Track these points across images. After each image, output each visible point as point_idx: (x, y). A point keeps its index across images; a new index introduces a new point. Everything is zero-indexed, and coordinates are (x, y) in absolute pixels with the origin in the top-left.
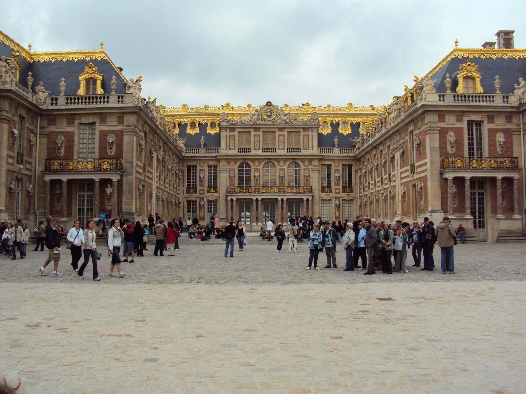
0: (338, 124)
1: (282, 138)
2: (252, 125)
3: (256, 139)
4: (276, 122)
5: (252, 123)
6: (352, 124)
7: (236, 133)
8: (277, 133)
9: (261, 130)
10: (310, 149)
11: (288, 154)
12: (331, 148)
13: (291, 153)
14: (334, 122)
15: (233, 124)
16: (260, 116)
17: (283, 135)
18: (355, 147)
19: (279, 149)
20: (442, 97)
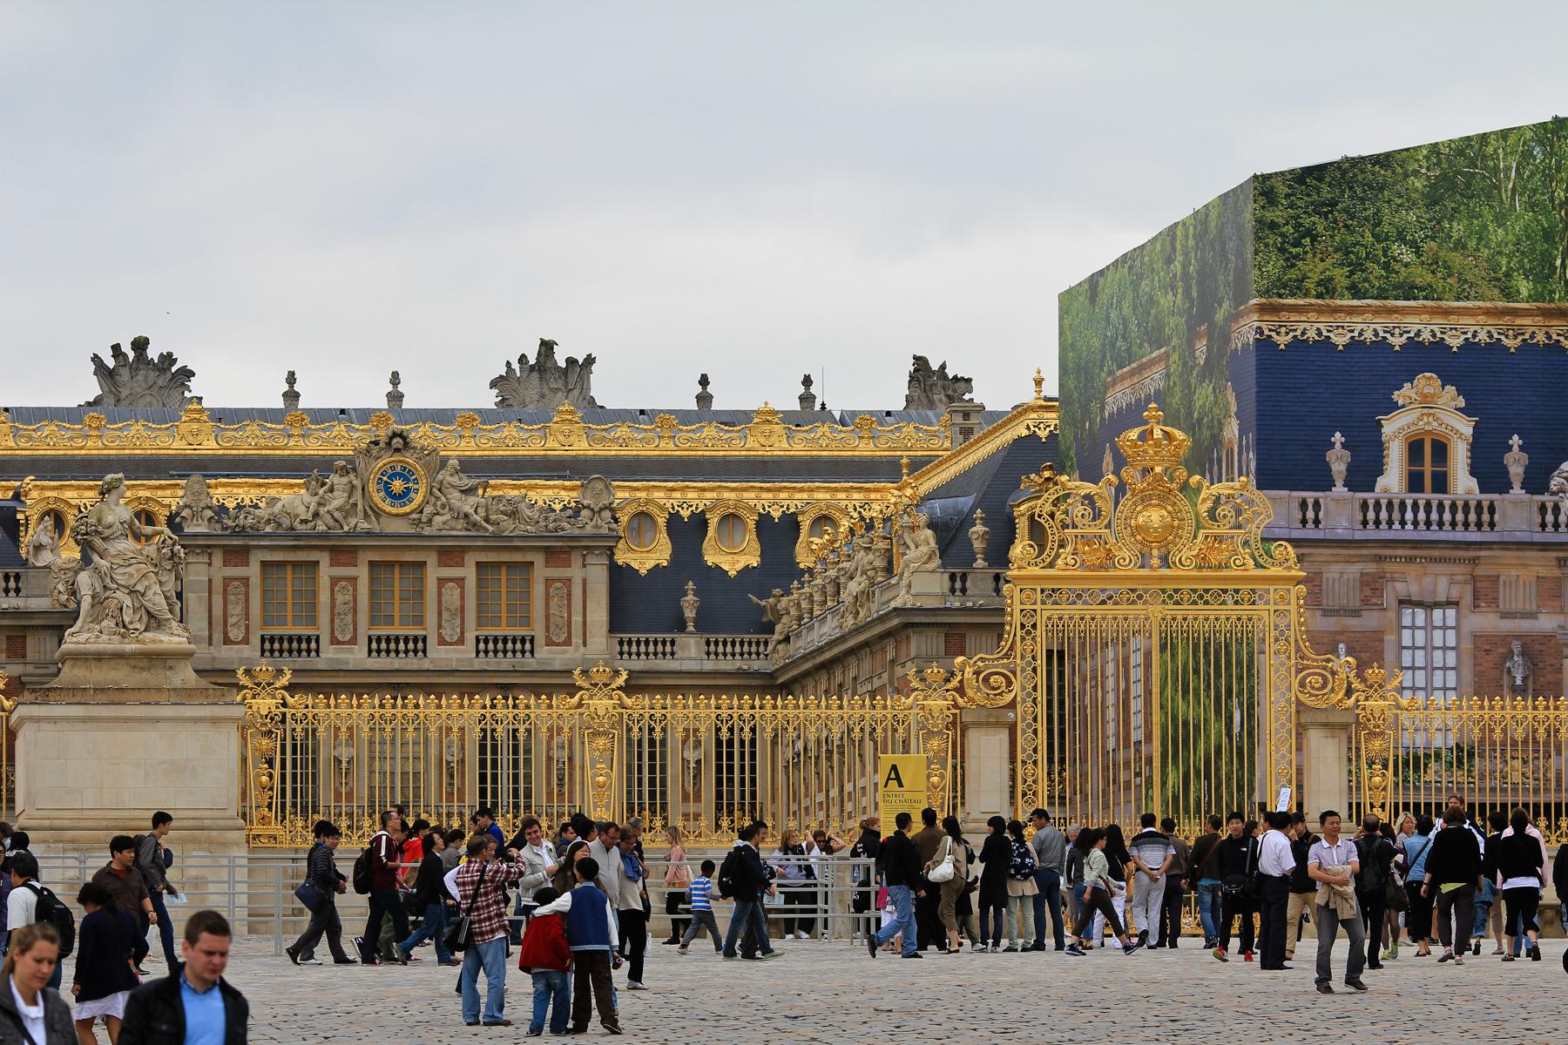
0: (700, 521)
1: (452, 595)
2: (321, 536)
3: (340, 598)
4: (430, 521)
5: (321, 528)
6: (764, 522)
7: (253, 571)
8: (433, 572)
9: (364, 558)
10: (577, 639)
11: (479, 663)
12: (668, 637)
13: (492, 663)
14: (685, 513)
15: (241, 532)
16: (358, 494)
17: (460, 581)
18: (769, 628)
19: (442, 641)
20: (958, 582)
